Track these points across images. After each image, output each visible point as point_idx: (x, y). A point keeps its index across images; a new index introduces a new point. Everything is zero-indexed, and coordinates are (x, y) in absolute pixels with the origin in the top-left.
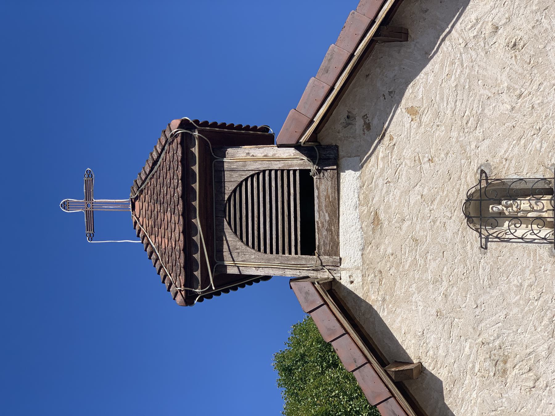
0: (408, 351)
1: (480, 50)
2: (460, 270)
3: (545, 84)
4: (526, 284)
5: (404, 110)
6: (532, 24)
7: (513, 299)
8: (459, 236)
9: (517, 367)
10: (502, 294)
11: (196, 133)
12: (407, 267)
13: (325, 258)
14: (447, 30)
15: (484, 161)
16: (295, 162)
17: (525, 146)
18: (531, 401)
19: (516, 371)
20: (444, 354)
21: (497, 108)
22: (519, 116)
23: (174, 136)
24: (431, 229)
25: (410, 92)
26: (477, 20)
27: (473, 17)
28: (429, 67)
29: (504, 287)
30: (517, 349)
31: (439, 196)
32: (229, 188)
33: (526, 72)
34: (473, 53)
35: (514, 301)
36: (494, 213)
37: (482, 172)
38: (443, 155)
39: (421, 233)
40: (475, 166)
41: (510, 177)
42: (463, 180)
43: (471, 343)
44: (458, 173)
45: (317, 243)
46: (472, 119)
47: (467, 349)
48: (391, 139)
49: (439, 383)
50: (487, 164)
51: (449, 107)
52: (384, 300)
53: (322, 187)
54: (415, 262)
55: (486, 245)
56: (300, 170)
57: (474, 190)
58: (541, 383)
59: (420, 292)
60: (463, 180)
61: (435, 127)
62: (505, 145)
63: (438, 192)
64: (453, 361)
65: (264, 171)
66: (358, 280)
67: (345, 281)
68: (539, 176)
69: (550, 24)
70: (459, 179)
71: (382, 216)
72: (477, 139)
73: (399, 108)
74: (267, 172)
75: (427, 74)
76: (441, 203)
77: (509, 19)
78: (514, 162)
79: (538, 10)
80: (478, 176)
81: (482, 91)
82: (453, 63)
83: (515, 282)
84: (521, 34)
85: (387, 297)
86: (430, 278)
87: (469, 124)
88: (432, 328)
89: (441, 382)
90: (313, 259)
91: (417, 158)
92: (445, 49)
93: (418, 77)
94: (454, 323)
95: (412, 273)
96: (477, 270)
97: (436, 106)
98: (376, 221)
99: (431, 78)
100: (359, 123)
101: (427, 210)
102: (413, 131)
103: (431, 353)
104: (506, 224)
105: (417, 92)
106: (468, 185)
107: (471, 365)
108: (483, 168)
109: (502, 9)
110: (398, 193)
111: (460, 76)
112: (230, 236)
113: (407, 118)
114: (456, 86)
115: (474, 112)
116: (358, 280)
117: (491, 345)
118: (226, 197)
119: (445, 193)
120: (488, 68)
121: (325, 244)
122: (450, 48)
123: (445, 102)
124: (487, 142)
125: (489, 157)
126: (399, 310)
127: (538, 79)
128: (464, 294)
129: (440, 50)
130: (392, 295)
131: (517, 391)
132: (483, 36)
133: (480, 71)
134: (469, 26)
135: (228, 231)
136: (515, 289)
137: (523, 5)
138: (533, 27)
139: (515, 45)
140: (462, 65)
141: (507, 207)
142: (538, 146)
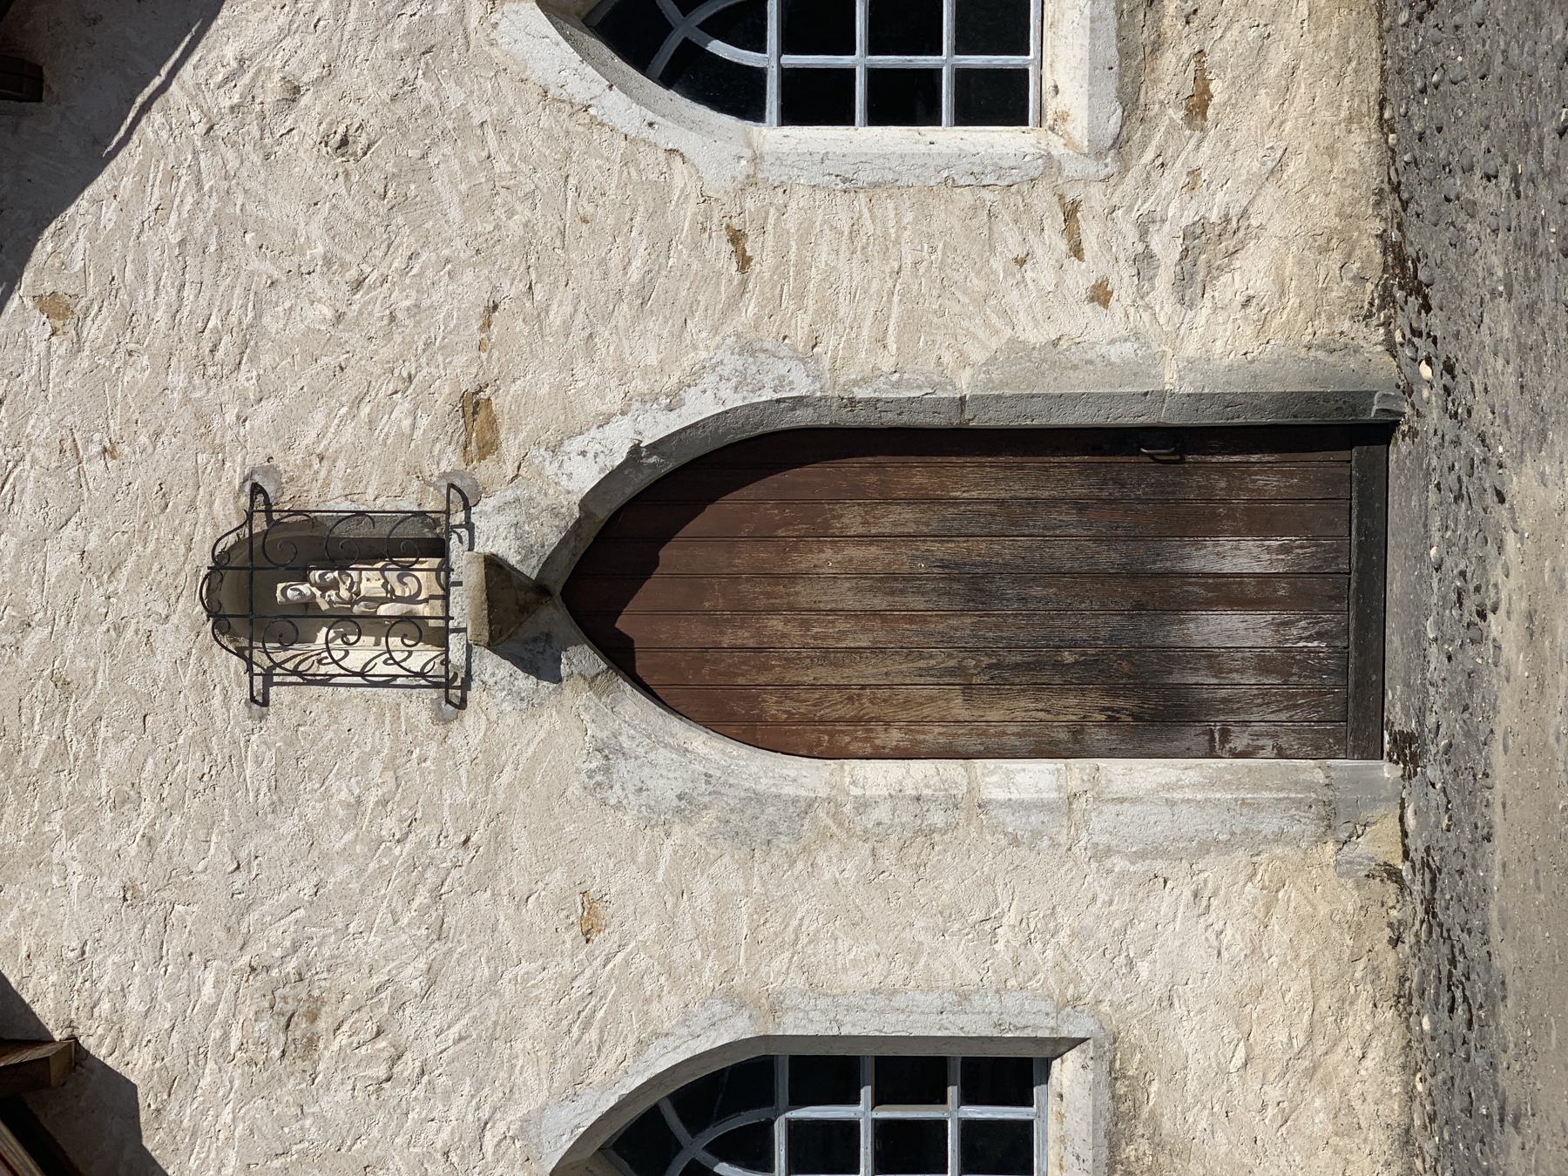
0: (36, 1008)
1: (249, 148)
2: (191, 765)
3: (424, 256)
4: (371, 799)
5: (29, 303)
6: (391, 89)
7: (336, 839)
8: (191, 670)
9: (345, 1027)
10: (309, 829)
12: (36, 763)
14: (157, 81)
15: (260, 460)
17: (371, 423)
18: (381, 1117)
19: (342, 1038)
20: (142, 1009)
21: (296, 315)
22: (355, 339)
24: (110, 651)
25: (49, 248)
26: (241, 61)
27: (230, 52)
28: (103, 182)
29: (314, 810)
30: (345, 977)
31: (134, 557)
33: (373, 221)
34: (230, 155)
35: (338, 846)
36: (289, 603)
37: (257, 489)
38: (143, 439)
39: (81, 663)
40: (234, 474)
41: (331, 505)
42: (202, 512)
43: (220, 970)
44: (189, 492)
46: (226, 339)
47: (208, 990)
49: (124, 1092)
50: (270, 470)
51: (163, 300)
54: (60, 747)
55: (266, 695)
57: (232, 539)
58: (409, 1066)
59: (75, 832)
60: (202, 512)
61: (121, 355)
62: (319, 417)
63: (129, 544)
64: (167, 1026)
68: (408, 504)
69: (437, 92)
70: (192, 507)
73: (16, 297)
75: (97, 202)
76: (139, 575)
77: (329, 69)
78: (341, 464)
79: (408, 51)
80: (245, 500)
81: (255, 264)
82: (173, 178)
83: (344, 795)
84: (362, 113)
86: (104, 792)
87: (219, 355)
88: (110, 935)
89: (134, 1087)
91: (68, 444)
92: (151, 136)
93: (72, 210)
94: (173, 919)
95: (51, 780)
96: (241, 766)
97: (123, 295)
99: (109, 213)
101: (97, 597)
102: (56, 365)
103: (105, 1006)
105: (69, 252)
106: (216, 526)
107: (218, 1033)
108: (257, 478)
109: (310, 39)
111: (192, 215)
114: (183, 242)
115: (233, 320)
117: (274, 973)
119: (151, 546)
120: (271, 199)
122: (164, 134)
123: (152, 287)
124: (269, 406)
125: (274, 449)
128: (201, 834)
129: (135, 137)
131: (343, 1095)
132: (258, 108)
133: (250, 208)
134: (220, 77)
136: (341, 813)
137: (367, 35)
138: (394, 98)
139: (344, 142)
140: (199, 184)
141: (324, 589)
142: (407, 423)
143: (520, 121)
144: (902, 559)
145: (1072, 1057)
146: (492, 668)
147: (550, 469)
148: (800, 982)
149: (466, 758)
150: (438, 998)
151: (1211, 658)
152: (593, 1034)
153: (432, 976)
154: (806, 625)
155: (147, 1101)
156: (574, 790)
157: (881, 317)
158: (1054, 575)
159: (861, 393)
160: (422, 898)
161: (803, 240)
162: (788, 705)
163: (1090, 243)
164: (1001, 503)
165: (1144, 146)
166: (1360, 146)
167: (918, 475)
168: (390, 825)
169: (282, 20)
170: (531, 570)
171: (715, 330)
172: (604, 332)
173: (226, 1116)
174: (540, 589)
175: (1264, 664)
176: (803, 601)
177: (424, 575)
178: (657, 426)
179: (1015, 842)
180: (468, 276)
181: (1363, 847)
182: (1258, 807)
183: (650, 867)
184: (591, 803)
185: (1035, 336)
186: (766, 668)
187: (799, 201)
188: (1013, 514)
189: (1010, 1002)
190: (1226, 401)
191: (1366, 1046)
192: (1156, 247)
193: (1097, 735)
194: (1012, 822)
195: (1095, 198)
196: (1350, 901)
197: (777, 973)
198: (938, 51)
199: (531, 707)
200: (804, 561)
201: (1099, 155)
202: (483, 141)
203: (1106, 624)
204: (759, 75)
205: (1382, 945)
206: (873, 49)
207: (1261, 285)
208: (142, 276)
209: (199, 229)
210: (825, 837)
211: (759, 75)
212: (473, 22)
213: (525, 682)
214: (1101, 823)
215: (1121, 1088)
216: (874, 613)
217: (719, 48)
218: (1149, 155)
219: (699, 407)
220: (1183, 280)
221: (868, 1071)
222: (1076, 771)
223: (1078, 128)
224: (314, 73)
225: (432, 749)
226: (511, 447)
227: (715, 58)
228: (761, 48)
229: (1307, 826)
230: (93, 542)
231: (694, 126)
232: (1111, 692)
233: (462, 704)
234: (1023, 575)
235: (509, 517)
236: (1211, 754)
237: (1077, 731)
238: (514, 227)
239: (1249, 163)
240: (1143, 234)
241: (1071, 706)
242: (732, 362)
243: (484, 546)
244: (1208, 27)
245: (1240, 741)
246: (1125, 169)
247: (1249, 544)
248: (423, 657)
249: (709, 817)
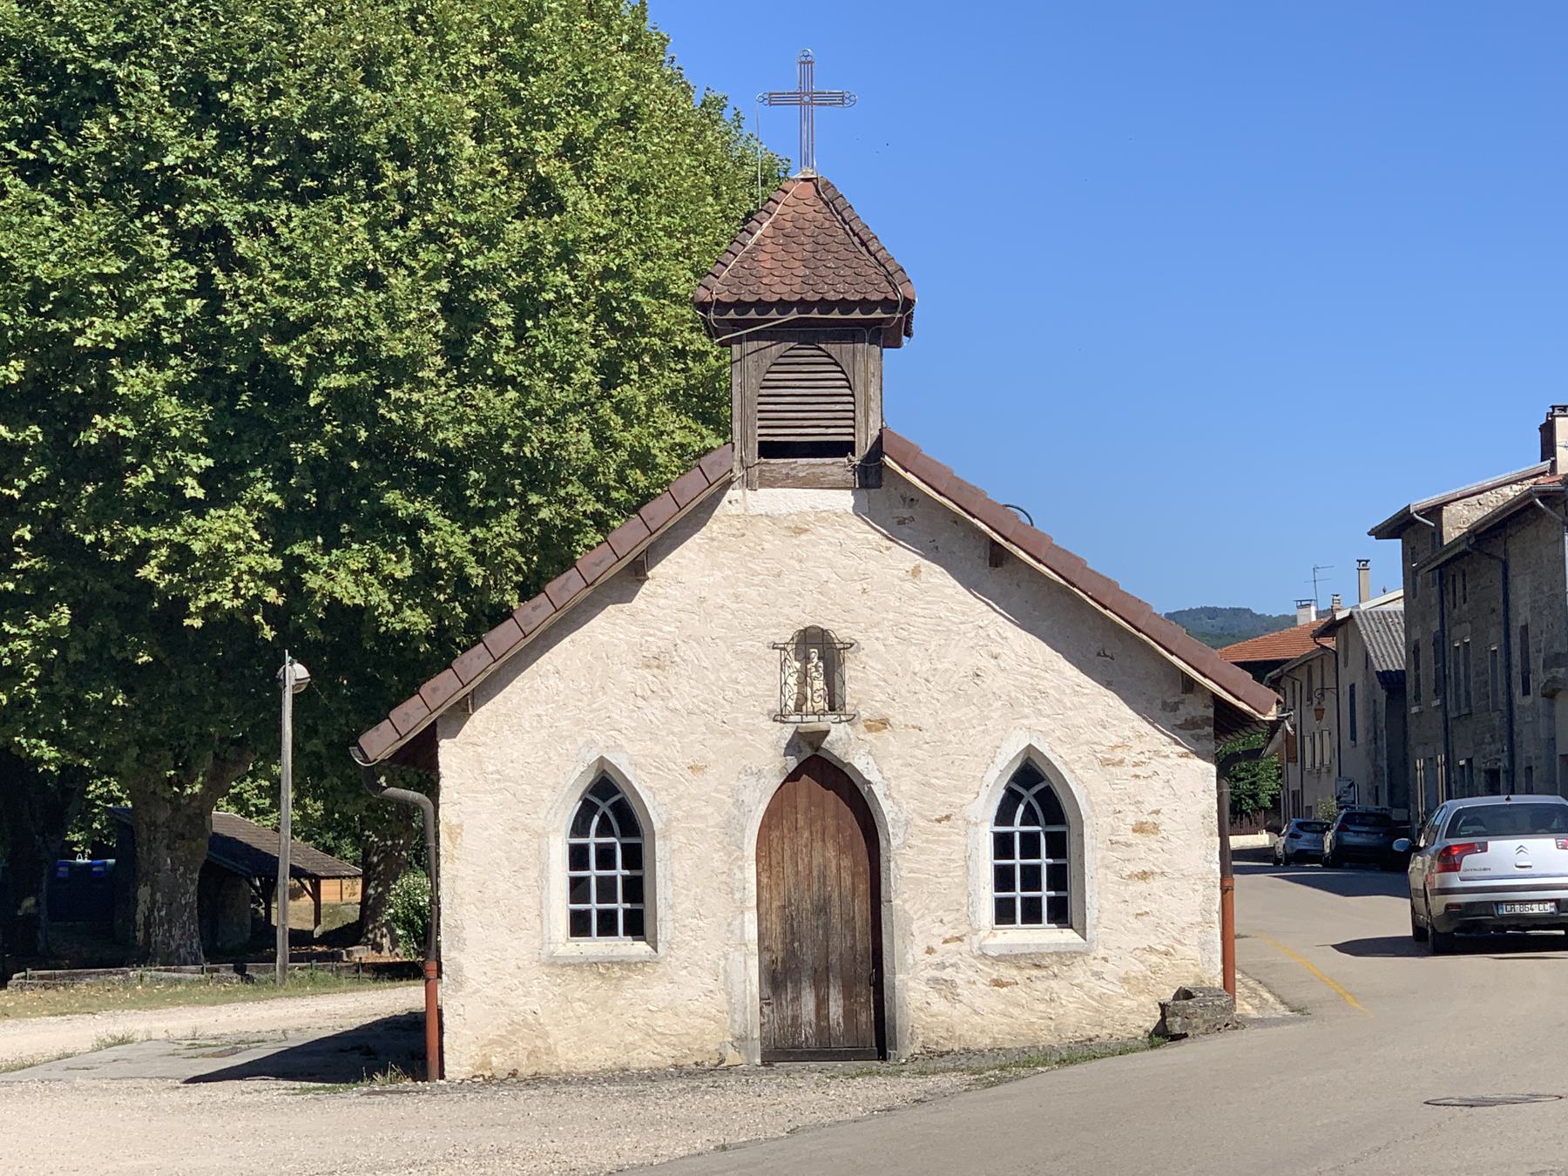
4: (739, 687)
6: (998, 692)
10: (728, 664)
11: (899, 316)
12: (750, 565)
13: (756, 471)
16: (863, 436)
17: (877, 686)
19: (650, 678)
22: (908, 679)
23: (895, 289)
27: (1008, 634)
29: (734, 666)
30: (673, 679)
32: (833, 349)
34: (973, 634)
37: (852, 645)
39: (786, 581)
45: (772, 461)
47: (668, 628)
48: (888, 549)
50: (859, 649)
52: (713, 539)
53: (835, 469)
54: (755, 574)
56: (854, 442)
58: (640, 703)
65: (852, 395)
66: (734, 510)
67: (731, 494)
71: (803, 537)
72: (885, 639)
74: (851, 399)
75: (955, 587)
76: (819, 602)
77: (1004, 670)
80: (848, 641)
81: (934, 643)
82: (964, 614)
84: (989, 682)
85: (715, 543)
88: (686, 592)
90: (754, 459)
98: (799, 531)
99: (949, 591)
100: (905, 513)
101: (811, 587)
102: (895, 572)
103: (660, 591)
104: (798, 665)
107: (651, 632)
110: (830, 555)
112: (776, 349)
113: (910, 566)
116: (734, 510)
118: (822, 346)
121: (771, 471)
124: (882, 649)
126: (702, 555)
127: (943, 698)
130: (718, 548)
131: (630, 679)
135: (784, 346)
137: (1017, 683)
141: (816, 666)
143: (988, 738)
144: (832, 880)
145: (649, 948)
146: (789, 730)
147: (862, 751)
148: (675, 847)
149: (756, 721)
150: (666, 713)
151: (797, 998)
152: (654, 770)
153: (673, 711)
154: (806, 846)
155: (626, 606)
156: (744, 762)
157: (918, 871)
158: (827, 937)
159: (892, 864)
160: (703, 707)
161: (948, 842)
162: (775, 840)
163: (947, 946)
164: (854, 918)
165: (984, 964)
166: (985, 1042)
167: (863, 887)
168: (729, 694)
169: (1021, 653)
170: (824, 745)
171: (914, 811)
172: (912, 770)
173: (621, 636)
174: (818, 748)
175: (795, 1018)
176: (815, 844)
177: (822, 704)
178: (878, 791)
179: (729, 925)
180: (932, 721)
181: (731, 1051)
182: (744, 1013)
183: (717, 791)
184: (739, 769)
185: (914, 928)
186: (789, 831)
187: (962, 840)
188: (849, 922)
189: (670, 925)
190: (892, 998)
191: (658, 1054)
192: (949, 970)
193: (767, 956)
194: (737, 923)
195: (965, 947)
196: (711, 1047)
197: (678, 839)
198: (1022, 890)
199: (775, 746)
200: (830, 844)
201: (980, 948)
202: (980, 725)
203: (808, 958)
204: (1012, 824)
205: (695, 1059)
206: (1023, 867)
207: (935, 1008)
208: (928, 603)
209: (947, 623)
210: (729, 854)
211: (1012, 824)
212: (1023, 721)
213: (784, 744)
214: (737, 956)
215: (640, 965)
216: (811, 872)
217: (1021, 808)
218: (981, 967)
219: (886, 806)
220: (936, 980)
221: (636, 873)
222: (754, 947)
223: (991, 941)
224: (1002, 665)
225: (758, 709)
226: (870, 737)
227: (1017, 807)
228: (1022, 824)
229: (738, 1031)
230: (831, 586)
231: (988, 801)
232: (783, 961)
233: (775, 720)
234: (827, 927)
235: (844, 736)
236: (761, 999)
237: (768, 949)
238: (949, 737)
239: (978, 1003)
240: (952, 965)
241: (778, 946)
242: (902, 817)
243: (833, 727)
244: (1026, 985)
245: (766, 1010)
246: (975, 958)
247: (841, 1011)
248: (791, 704)
249: (736, 812)
